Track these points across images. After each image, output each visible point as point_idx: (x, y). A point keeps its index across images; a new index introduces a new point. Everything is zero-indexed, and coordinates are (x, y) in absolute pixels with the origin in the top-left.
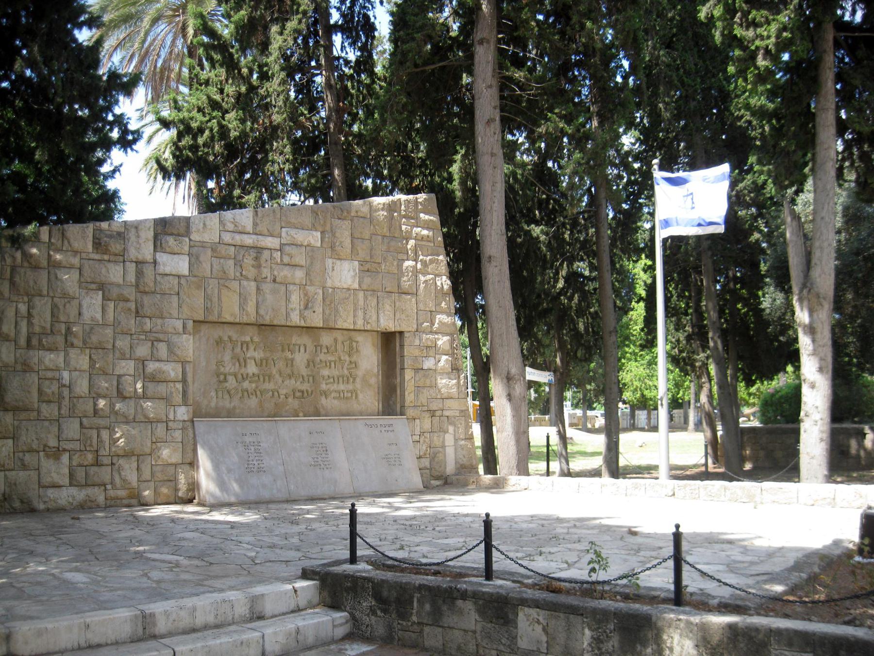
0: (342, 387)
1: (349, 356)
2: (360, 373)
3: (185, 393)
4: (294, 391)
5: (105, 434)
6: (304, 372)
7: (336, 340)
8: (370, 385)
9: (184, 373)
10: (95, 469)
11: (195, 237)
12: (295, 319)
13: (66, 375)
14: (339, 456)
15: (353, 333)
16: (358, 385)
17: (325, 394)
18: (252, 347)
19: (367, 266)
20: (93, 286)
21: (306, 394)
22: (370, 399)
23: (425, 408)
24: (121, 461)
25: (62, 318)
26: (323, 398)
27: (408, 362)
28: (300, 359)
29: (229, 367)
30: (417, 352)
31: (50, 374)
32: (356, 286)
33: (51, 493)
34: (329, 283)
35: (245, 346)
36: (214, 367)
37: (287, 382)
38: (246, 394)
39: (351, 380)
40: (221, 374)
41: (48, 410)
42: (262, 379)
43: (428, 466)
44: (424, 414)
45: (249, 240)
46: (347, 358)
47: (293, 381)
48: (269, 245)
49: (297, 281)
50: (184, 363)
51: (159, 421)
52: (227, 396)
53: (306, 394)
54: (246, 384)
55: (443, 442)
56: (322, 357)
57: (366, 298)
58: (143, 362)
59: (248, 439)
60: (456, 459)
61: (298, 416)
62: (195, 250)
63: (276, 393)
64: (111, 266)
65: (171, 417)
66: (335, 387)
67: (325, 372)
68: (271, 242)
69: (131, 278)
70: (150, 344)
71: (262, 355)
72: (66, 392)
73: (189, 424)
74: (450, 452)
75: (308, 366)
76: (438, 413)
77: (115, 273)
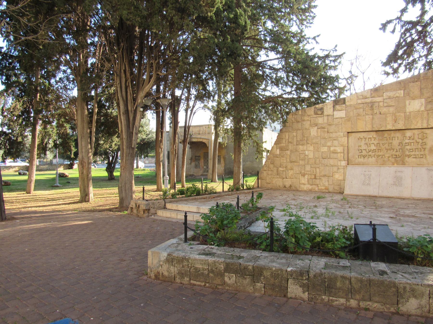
0: (417, 153)
1: (422, 140)
2: (428, 147)
4: (392, 155)
7: (414, 134)
9: (344, 150)
10: (314, 180)
11: (347, 103)
12: (389, 127)
13: (307, 152)
16: (427, 152)
17: (409, 156)
18: (373, 139)
20: (314, 125)
21: (398, 157)
24: (323, 178)
25: (306, 136)
26: (407, 158)
28: (396, 142)
31: (302, 152)
32: (423, 108)
33: (302, 186)
34: (407, 110)
35: (370, 139)
39: (423, 150)
41: (301, 162)
45: (368, 100)
46: (420, 141)
48: (378, 100)
51: (335, 166)
52: (362, 158)
53: (398, 157)
54: (370, 153)
57: (428, 114)
58: (329, 147)
62: (347, 109)
64: (319, 118)
66: (413, 153)
67: (408, 147)
69: (326, 121)
70: (332, 141)
71: (377, 142)
72: (306, 157)
77: (320, 120)
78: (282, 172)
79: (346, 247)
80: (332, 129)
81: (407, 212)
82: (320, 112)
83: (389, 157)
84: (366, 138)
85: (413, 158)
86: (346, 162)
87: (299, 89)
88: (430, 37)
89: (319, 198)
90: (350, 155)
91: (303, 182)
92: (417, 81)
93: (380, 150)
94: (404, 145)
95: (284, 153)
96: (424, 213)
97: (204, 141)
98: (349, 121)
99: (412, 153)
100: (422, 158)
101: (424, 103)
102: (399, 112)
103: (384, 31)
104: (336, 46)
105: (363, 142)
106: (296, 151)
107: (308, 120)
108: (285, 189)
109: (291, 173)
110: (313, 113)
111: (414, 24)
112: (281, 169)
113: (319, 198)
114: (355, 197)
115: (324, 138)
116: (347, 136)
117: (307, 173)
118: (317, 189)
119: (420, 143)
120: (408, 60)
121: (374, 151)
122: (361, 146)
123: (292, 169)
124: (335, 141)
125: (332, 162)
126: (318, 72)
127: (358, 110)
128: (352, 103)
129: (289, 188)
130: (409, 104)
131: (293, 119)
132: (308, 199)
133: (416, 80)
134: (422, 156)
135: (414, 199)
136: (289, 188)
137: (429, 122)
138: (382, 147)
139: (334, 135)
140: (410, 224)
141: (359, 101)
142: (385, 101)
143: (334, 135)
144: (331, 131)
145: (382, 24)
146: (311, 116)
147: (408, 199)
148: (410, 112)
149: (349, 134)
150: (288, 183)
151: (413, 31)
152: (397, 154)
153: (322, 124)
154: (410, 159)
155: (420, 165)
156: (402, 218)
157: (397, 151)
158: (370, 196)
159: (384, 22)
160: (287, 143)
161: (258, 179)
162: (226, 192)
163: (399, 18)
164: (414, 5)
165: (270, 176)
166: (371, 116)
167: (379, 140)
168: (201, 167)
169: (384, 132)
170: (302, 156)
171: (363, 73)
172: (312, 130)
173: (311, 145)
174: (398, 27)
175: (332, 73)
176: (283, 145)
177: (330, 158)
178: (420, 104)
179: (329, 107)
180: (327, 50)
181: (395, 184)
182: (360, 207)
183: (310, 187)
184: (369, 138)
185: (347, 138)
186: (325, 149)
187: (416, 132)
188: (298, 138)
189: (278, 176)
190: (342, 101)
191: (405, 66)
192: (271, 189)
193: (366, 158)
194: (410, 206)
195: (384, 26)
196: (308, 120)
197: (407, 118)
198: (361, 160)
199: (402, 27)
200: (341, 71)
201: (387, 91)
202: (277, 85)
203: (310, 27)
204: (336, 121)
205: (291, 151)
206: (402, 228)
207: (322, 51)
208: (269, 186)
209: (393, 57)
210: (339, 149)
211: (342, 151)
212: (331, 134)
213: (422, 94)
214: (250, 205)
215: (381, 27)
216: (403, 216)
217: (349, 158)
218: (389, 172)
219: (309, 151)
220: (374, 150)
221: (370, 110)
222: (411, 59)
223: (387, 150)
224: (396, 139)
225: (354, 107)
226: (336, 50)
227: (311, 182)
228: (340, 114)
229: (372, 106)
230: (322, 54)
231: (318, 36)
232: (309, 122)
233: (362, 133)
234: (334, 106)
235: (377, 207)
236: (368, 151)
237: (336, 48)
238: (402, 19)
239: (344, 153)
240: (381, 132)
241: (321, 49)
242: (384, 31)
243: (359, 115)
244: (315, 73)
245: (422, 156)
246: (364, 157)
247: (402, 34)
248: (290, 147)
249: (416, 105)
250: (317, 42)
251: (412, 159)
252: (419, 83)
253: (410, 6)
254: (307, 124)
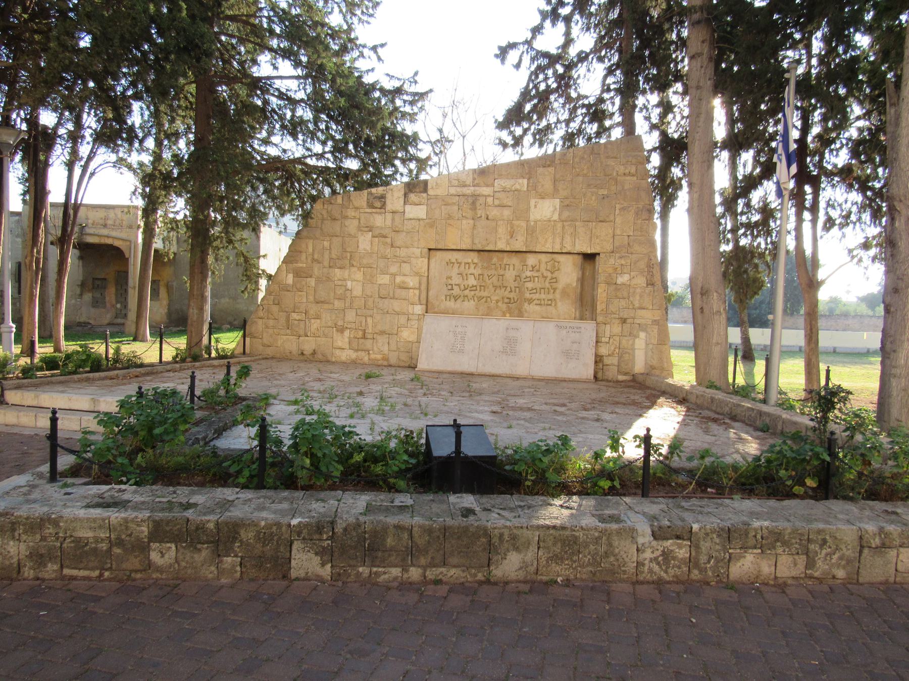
0: (543, 296)
1: (552, 273)
2: (560, 286)
5: (370, 320)
9: (420, 284)
10: (361, 341)
11: (430, 192)
12: (501, 246)
13: (349, 284)
15: (555, 256)
16: (558, 295)
17: (530, 301)
18: (472, 266)
19: (567, 202)
20: (366, 229)
24: (378, 337)
25: (349, 249)
26: (526, 304)
28: (510, 274)
29: (456, 280)
31: (340, 283)
32: (556, 217)
33: (337, 352)
34: (532, 218)
41: (338, 304)
43: (616, 363)
44: (614, 321)
45: (469, 191)
46: (549, 275)
47: (503, 289)
48: (484, 193)
49: (505, 217)
52: (453, 300)
55: (633, 344)
56: (529, 274)
57: (563, 227)
58: (394, 275)
60: (646, 360)
62: (430, 202)
64: (376, 216)
66: (537, 296)
67: (530, 285)
68: (486, 191)
70: (398, 265)
71: (480, 272)
72: (348, 293)
76: (628, 321)
77: (379, 220)
78: (296, 322)
79: (408, 470)
80: (400, 239)
81: (521, 401)
82: (378, 204)
83: (497, 301)
84: (460, 263)
86: (424, 307)
87: (339, 149)
88: (576, 89)
89: (368, 377)
90: (430, 293)
91: (339, 344)
92: (549, 166)
93: (483, 287)
95: (304, 283)
96: (546, 404)
97: (117, 243)
98: (432, 225)
101: (558, 207)
102: (518, 220)
103: (503, 61)
104: (416, 74)
105: (456, 270)
106: (329, 279)
107: (355, 218)
108: (301, 358)
109: (315, 324)
110: (364, 204)
111: (553, 59)
112: (295, 316)
113: (368, 377)
114: (436, 375)
115: (385, 257)
116: (427, 256)
117: (349, 326)
118: (366, 359)
120: (538, 125)
121: (473, 288)
122: (450, 278)
123: (318, 317)
124: (404, 265)
125: (396, 305)
126: (378, 120)
127: (449, 207)
128: (439, 192)
129: (311, 358)
130: (535, 206)
131: (324, 212)
132: (346, 378)
133: (548, 163)
135: (533, 379)
136: (311, 358)
137: (564, 242)
138: (487, 280)
139: (403, 253)
140: (522, 422)
141: (453, 191)
142: (497, 195)
143: (403, 253)
144: (398, 243)
145: (500, 48)
146: (362, 211)
147: (525, 378)
148: (536, 222)
149: (432, 252)
150: (308, 345)
151: (550, 72)
152: (512, 295)
153: (382, 228)
155: (546, 318)
156: (511, 413)
157: (511, 291)
158: (462, 373)
159: (504, 44)
160: (309, 261)
161: (244, 336)
162: (168, 363)
163: (528, 43)
164: (554, 24)
165: (271, 331)
166: (471, 222)
167: (483, 268)
168: (108, 305)
169: (491, 254)
170: (340, 291)
171: (464, 137)
172: (361, 239)
173: (359, 269)
174: (526, 60)
175: (406, 127)
176: (301, 265)
177: (394, 298)
178: (552, 209)
179: (396, 194)
180: (399, 79)
181: (504, 352)
182: (443, 393)
183: (354, 355)
184: (466, 263)
185: (426, 260)
186: (385, 279)
187: (543, 257)
188: (333, 252)
189: (288, 331)
190: (422, 185)
191: (534, 135)
192: (272, 358)
193: (459, 301)
194: (526, 390)
195: (503, 52)
196: (355, 218)
197: (531, 231)
198: (451, 304)
199: (533, 60)
200: (423, 126)
201: (500, 176)
202: (294, 136)
203: (368, 23)
204: (408, 226)
205: (319, 280)
206: (510, 431)
207: (388, 78)
208: (269, 352)
209: (515, 116)
210: (412, 282)
211: (417, 286)
212: (398, 249)
213: (556, 190)
214: (222, 392)
215: (498, 52)
216: (514, 409)
217: (430, 298)
218: (496, 328)
219: (354, 282)
220: (473, 286)
221: (471, 209)
222: (544, 123)
223: (495, 287)
224: (511, 268)
225: (443, 200)
226: (416, 82)
227: (355, 345)
228: (417, 212)
229: (474, 203)
230: (389, 85)
231: (382, 45)
232: (356, 222)
233: (455, 253)
234: (405, 195)
235: (472, 394)
236: (462, 287)
237: (416, 78)
238: (534, 46)
239: (419, 289)
240: (486, 253)
241: (388, 75)
242: (503, 61)
243: (450, 217)
244: (372, 122)
245: (552, 302)
246: (456, 298)
247: (532, 73)
248: (316, 271)
249: (545, 209)
250: (379, 59)
252: (551, 170)
253: (548, 23)
254: (352, 226)
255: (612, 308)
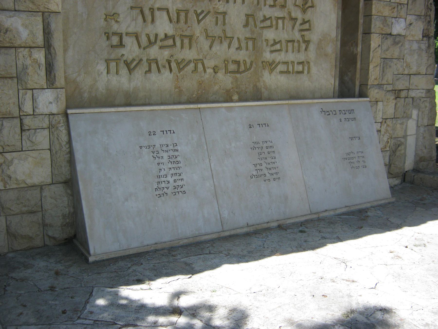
0: (291, 57)
1: (304, 11)
2: (314, 37)
3: (50, 68)
4: (226, 62)
6: (241, 33)
8: (326, 55)
9: (47, 33)
14: (288, 159)
16: (312, 54)
17: (271, 66)
22: (324, 75)
23: (390, 88)
26: (266, 74)
27: (376, 25)
30: (386, 12)
36: (102, 23)
37: (216, 48)
38: (154, 66)
39: (303, 46)
40: (114, 34)
42: (178, 43)
46: (297, 14)
47: (225, 44)
50: (46, 16)
52: (124, 71)
53: (242, 68)
56: (267, 12)
59: (158, 141)
60: (416, 150)
61: (232, 101)
63: (200, 66)
65: (28, 108)
66: (280, 57)
67: (270, 35)
73: (61, 118)
74: (411, 142)
75: (246, 25)
85: (281, 72)
94: (258, 23)
99: (280, 57)
100: (302, 72)
119: (299, 22)
134: (300, 68)
154: (273, 76)
157: (239, 48)
193: (139, 74)
220: (166, 36)
236: (144, 41)
251: (279, 77)
255: (389, 77)
